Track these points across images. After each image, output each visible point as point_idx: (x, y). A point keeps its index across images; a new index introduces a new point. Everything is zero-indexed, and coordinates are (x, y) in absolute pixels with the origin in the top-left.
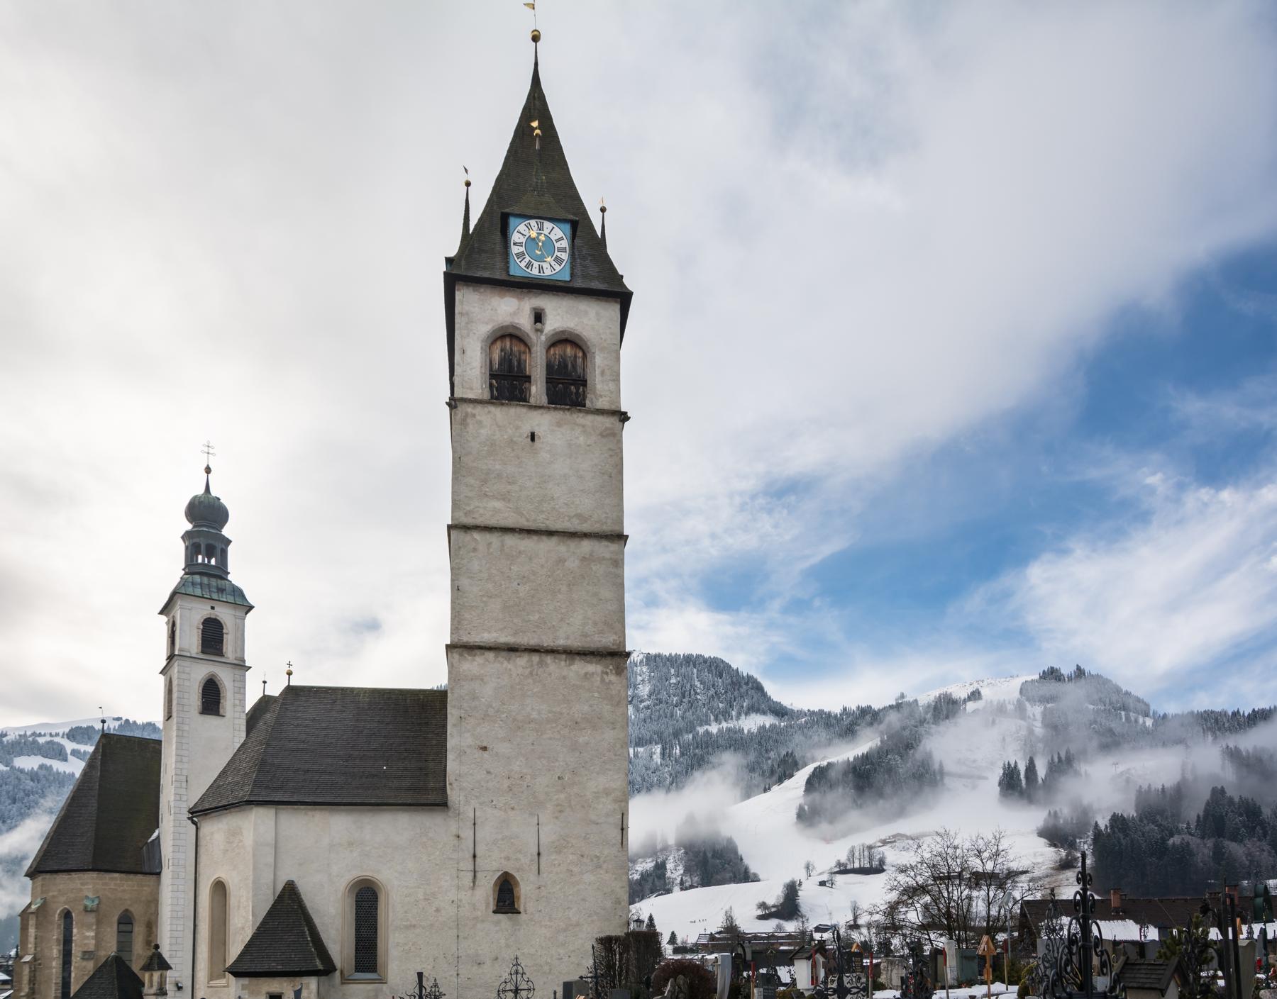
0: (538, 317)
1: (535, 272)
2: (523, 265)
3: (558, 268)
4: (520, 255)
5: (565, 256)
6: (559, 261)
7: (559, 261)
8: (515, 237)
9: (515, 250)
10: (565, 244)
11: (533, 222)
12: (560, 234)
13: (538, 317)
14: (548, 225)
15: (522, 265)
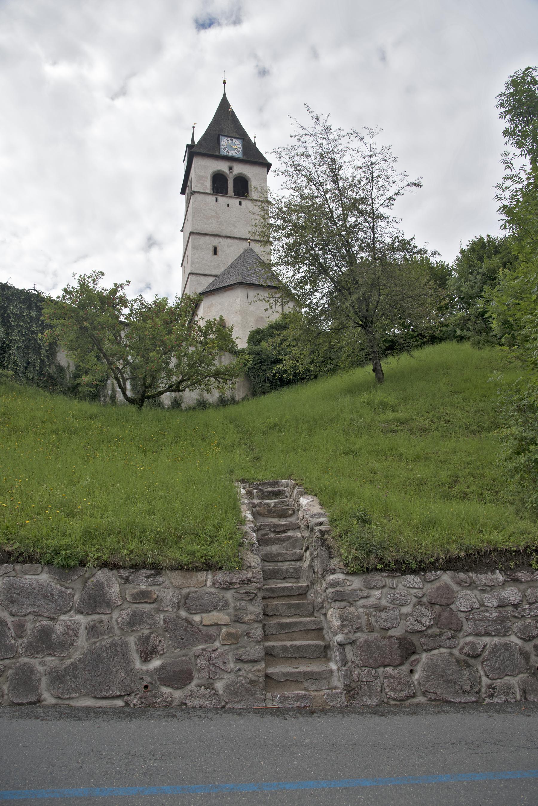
0: (231, 168)
1: (230, 154)
2: (225, 151)
3: (238, 153)
4: (224, 149)
5: (240, 150)
6: (238, 151)
7: (238, 151)
8: (222, 143)
9: (222, 147)
10: (240, 146)
11: (229, 139)
12: (238, 143)
13: (231, 168)
14: (234, 140)
15: (224, 152)
